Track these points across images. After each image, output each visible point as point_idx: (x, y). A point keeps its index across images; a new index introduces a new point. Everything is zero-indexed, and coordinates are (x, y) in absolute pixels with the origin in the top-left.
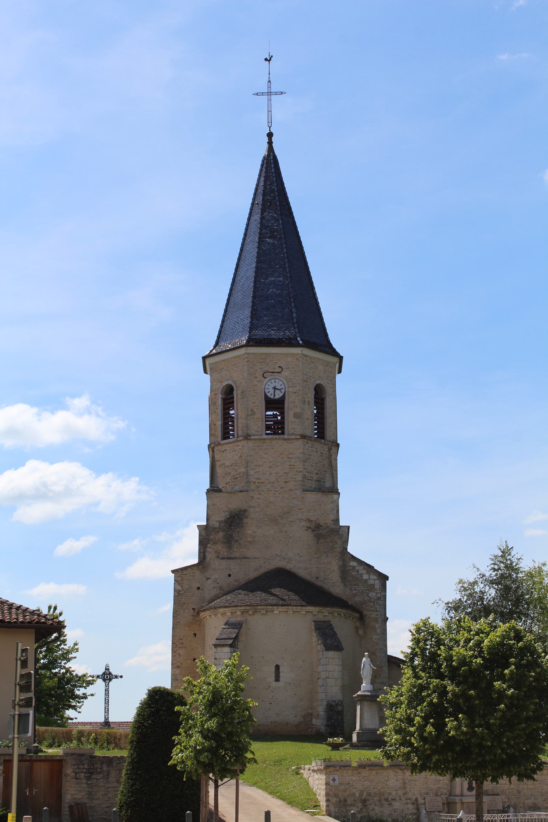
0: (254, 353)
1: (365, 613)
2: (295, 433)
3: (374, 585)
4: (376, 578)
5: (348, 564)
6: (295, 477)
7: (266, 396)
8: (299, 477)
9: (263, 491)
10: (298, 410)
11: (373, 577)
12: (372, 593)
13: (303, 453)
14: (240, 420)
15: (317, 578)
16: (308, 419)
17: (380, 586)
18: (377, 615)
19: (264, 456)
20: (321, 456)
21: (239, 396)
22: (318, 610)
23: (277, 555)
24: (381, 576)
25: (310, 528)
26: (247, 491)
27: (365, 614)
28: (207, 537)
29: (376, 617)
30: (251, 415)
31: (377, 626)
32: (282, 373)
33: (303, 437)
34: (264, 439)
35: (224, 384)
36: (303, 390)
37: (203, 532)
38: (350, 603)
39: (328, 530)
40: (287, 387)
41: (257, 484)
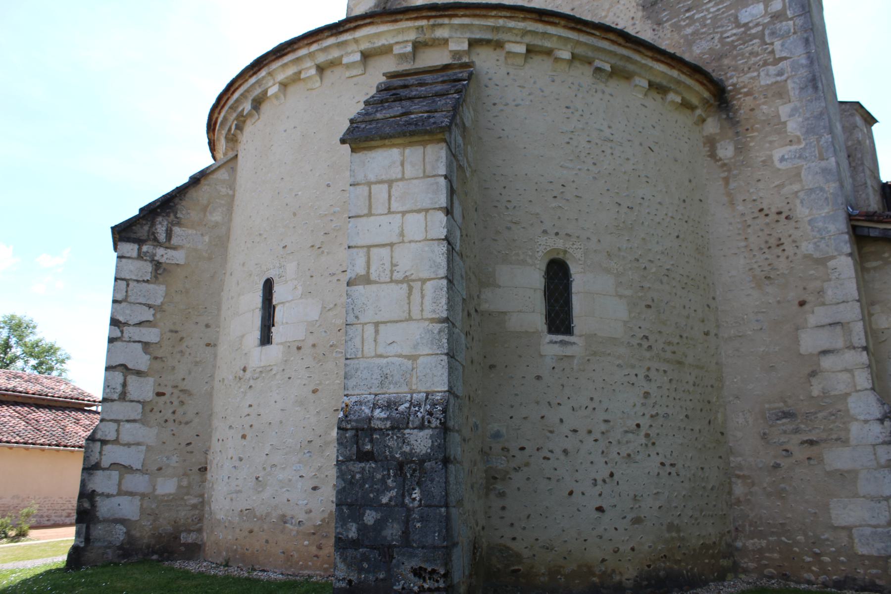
1: (735, 80)
18: (780, 74)
22: (412, 36)
27: (734, 85)
29: (777, 82)
31: (784, 110)
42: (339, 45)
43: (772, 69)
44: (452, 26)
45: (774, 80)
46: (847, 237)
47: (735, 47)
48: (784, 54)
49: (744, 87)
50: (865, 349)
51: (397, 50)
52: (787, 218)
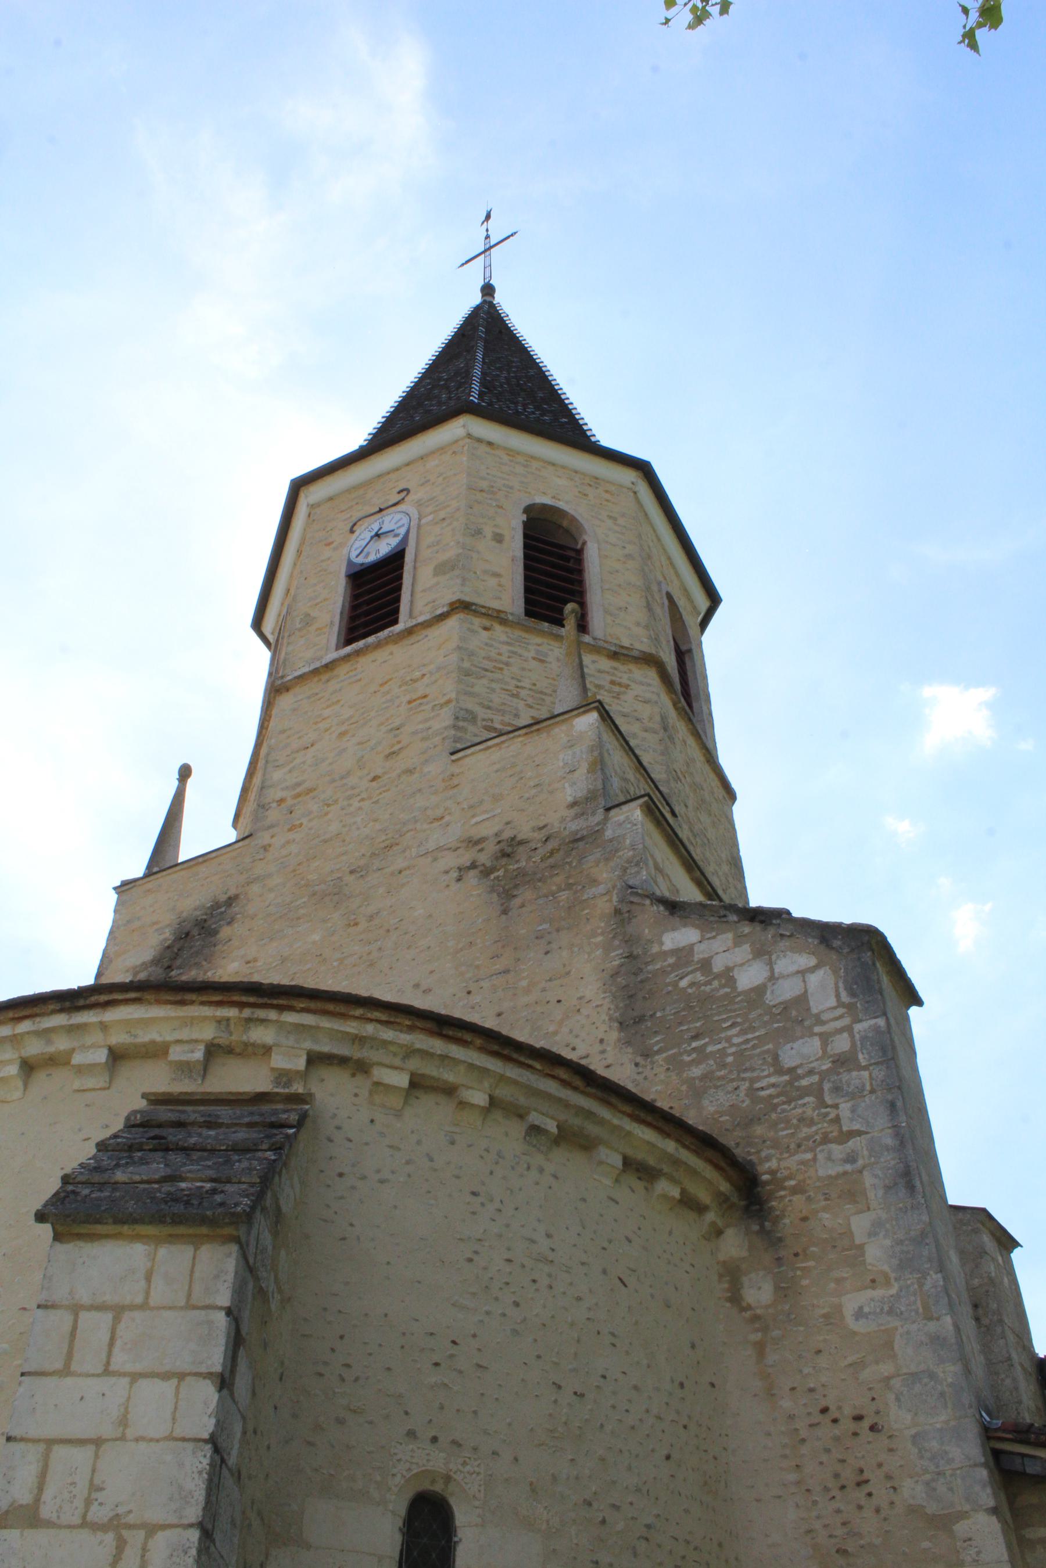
0: (331, 499)
1: (773, 1164)
3: (802, 1000)
4: (812, 961)
5: (655, 949)
6: (427, 725)
12: (796, 1045)
17: (838, 996)
18: (851, 1159)
22: (208, 1033)
24: (837, 943)
25: (473, 866)
27: (773, 1172)
29: (845, 1173)
31: (860, 1224)
41: (290, 802)
42: (71, 1029)
43: (837, 1150)
44: (281, 1025)
45: (840, 1169)
46: (983, 1473)
47: (776, 1106)
48: (856, 1126)
49: (790, 1178)
51: (176, 1054)
52: (873, 1428)
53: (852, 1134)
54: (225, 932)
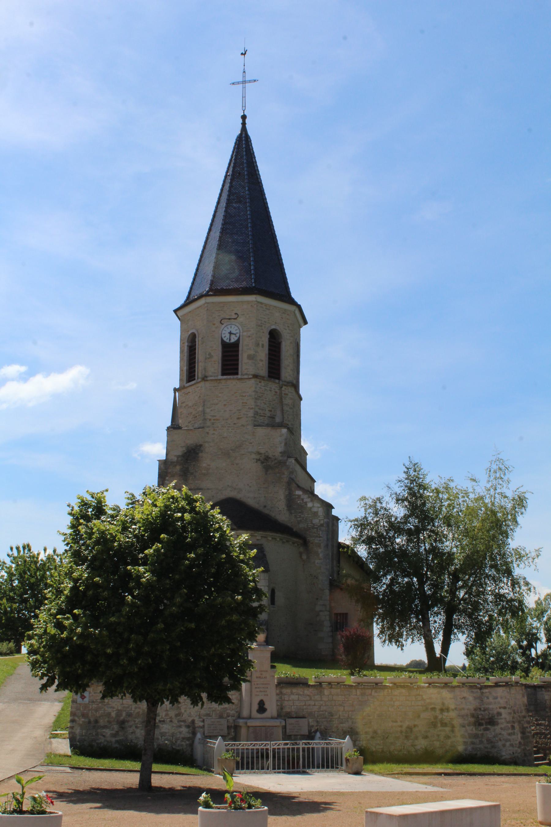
0: (213, 303)
1: (309, 538)
2: (248, 373)
4: (320, 506)
7: (222, 340)
8: (251, 414)
9: (218, 427)
10: (252, 352)
11: (317, 505)
13: (255, 391)
14: (200, 364)
15: (265, 507)
16: (262, 361)
18: (320, 541)
19: (220, 395)
20: (275, 395)
21: (200, 343)
23: (228, 485)
25: (259, 460)
26: (203, 428)
28: (165, 471)
30: (208, 358)
31: (320, 551)
32: (238, 319)
33: (255, 376)
34: (220, 380)
35: (190, 333)
36: (256, 334)
37: (162, 466)
38: (294, 530)
39: (276, 461)
40: (241, 331)
41: (213, 421)
43: (319, 539)
48: (322, 536)
50: (329, 611)
52: (317, 578)
53: (321, 537)
54: (200, 454)
